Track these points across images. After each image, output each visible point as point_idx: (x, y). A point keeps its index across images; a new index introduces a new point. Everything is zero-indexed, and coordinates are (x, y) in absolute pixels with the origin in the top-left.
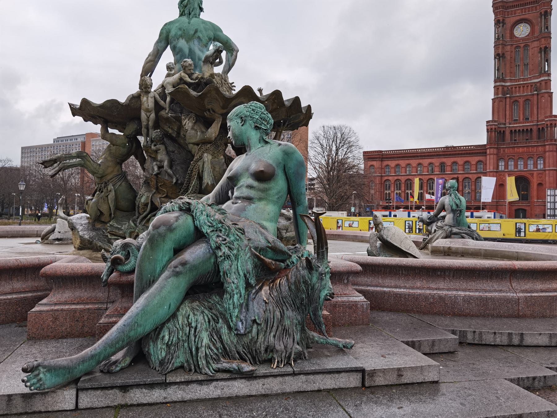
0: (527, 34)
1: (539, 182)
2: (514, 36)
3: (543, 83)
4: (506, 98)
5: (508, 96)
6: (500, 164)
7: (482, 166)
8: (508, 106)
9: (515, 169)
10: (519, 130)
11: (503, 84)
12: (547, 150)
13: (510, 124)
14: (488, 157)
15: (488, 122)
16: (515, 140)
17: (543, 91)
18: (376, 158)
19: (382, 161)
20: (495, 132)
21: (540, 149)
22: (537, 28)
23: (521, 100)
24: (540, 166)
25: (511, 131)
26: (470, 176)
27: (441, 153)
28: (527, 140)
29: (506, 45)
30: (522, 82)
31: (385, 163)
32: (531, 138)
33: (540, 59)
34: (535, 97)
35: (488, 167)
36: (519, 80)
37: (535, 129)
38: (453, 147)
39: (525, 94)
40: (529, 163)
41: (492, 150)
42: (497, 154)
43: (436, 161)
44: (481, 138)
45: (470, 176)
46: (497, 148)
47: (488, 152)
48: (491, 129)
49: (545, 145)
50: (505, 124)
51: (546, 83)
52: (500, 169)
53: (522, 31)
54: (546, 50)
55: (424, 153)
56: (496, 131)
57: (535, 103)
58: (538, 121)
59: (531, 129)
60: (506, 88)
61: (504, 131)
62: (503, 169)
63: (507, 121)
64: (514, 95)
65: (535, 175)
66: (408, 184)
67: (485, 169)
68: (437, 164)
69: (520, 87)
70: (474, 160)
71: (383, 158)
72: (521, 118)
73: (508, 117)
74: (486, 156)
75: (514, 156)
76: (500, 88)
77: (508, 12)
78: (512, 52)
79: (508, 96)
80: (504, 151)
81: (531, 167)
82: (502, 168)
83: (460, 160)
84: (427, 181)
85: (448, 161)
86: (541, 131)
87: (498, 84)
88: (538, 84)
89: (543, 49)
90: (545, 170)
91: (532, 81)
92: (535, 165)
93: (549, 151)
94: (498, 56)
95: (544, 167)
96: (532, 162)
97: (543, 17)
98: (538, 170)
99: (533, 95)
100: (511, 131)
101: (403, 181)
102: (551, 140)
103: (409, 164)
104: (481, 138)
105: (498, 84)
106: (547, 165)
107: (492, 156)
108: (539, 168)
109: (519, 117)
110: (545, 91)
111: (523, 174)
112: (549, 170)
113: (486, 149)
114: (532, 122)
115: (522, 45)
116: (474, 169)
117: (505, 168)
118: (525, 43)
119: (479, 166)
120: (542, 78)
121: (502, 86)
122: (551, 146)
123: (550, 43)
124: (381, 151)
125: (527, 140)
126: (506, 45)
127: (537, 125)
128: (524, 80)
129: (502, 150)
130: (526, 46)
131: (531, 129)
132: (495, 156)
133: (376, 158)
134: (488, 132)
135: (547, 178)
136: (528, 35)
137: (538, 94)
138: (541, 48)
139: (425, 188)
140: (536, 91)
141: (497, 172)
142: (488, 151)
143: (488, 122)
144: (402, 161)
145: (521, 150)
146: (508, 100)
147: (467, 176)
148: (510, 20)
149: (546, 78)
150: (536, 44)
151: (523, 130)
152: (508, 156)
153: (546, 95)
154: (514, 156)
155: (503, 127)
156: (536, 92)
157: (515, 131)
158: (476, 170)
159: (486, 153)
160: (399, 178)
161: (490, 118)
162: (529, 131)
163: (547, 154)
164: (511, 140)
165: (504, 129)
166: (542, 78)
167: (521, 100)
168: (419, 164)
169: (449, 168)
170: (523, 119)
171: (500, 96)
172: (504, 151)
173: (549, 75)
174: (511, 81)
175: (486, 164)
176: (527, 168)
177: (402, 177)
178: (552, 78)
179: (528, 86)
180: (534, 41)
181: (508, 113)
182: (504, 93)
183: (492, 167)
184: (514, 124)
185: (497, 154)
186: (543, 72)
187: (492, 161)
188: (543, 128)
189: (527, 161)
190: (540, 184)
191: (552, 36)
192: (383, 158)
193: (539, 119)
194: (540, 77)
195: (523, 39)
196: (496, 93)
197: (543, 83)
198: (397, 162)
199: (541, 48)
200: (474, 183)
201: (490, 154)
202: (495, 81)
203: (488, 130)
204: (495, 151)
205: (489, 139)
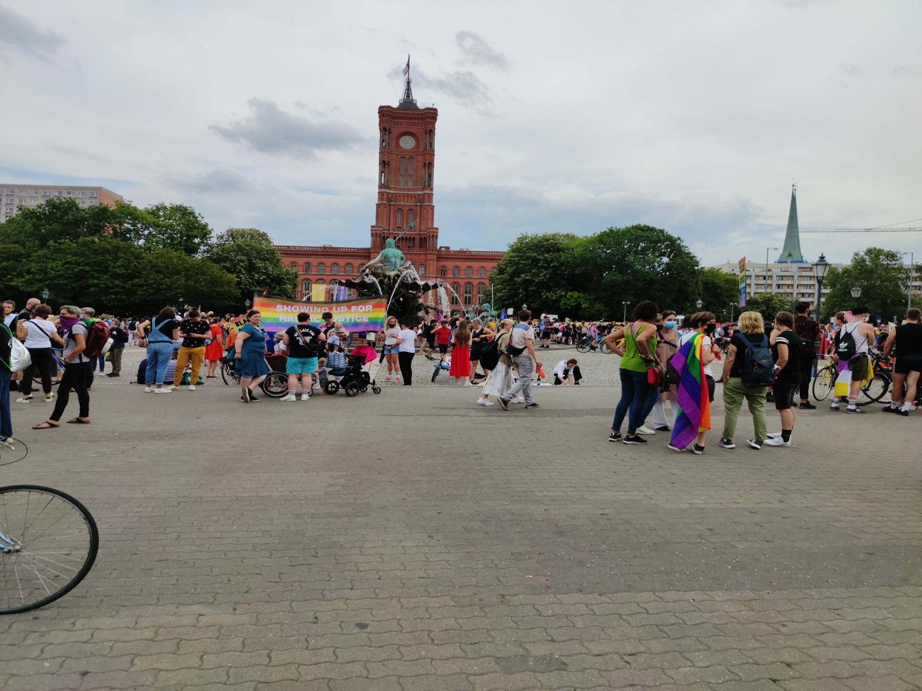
15: (372, 227)
21: (422, 257)
23: (405, 209)
34: (419, 208)
36: (403, 190)
37: (417, 238)
44: (366, 242)
53: (407, 143)
54: (430, 165)
70: (356, 262)
87: (383, 190)
94: (384, 164)
104: (366, 242)
105: (383, 190)
115: (407, 157)
118: (409, 156)
128: (408, 190)
146: (392, 207)
148: (396, 131)
161: (374, 224)
167: (405, 209)
174: (395, 189)
181: (392, 219)
182: (389, 200)
195: (408, 151)
202: (380, 187)
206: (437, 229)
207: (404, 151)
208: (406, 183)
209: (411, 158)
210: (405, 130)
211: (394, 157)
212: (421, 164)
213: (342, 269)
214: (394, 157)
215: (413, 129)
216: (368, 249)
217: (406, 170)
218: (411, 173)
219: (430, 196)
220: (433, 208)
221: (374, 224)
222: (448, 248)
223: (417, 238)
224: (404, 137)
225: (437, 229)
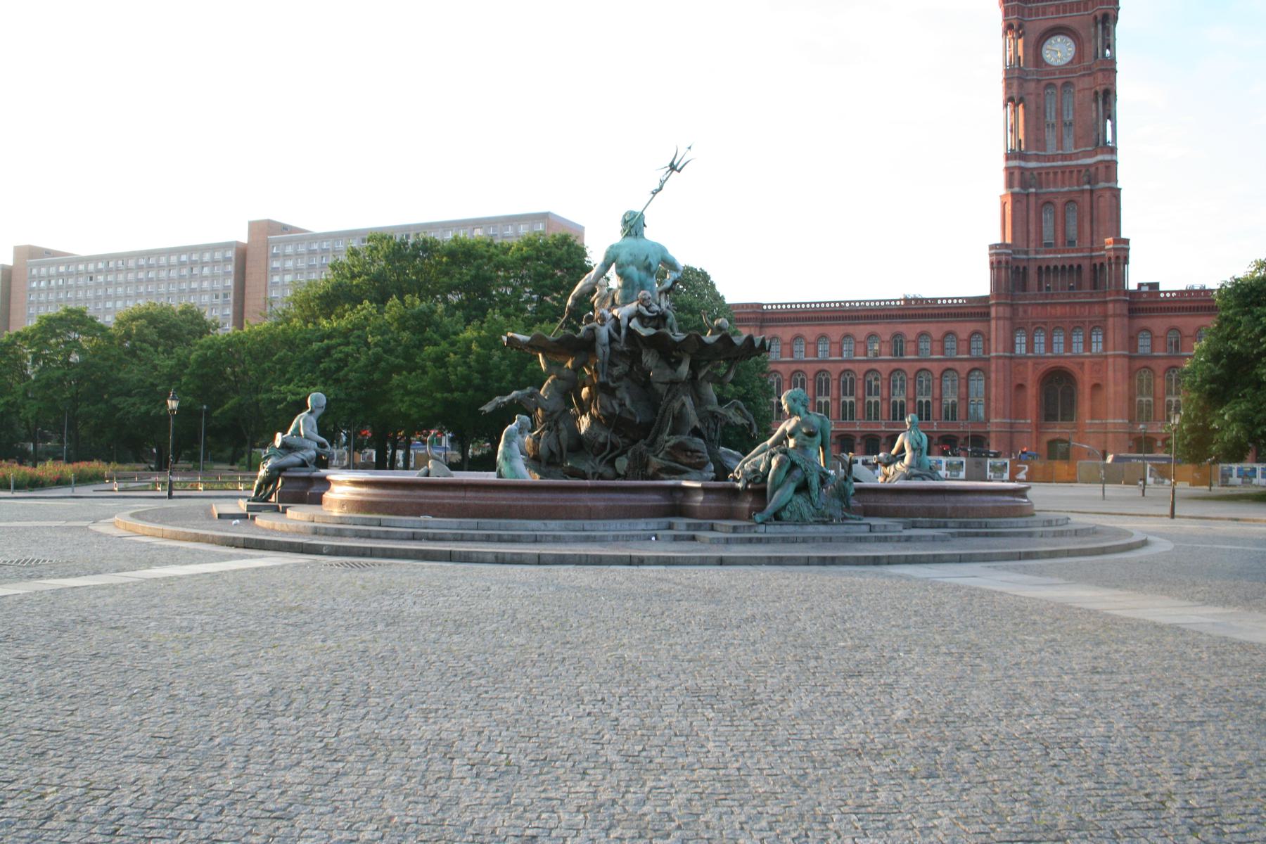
0: (1069, 59)
1: (1095, 381)
2: (1043, 61)
3: (1101, 167)
4: (1028, 195)
5: (1033, 190)
6: (1018, 340)
7: (980, 344)
8: (1032, 214)
9: (1046, 351)
10: (1056, 267)
11: (1023, 164)
12: (1110, 312)
13: (1037, 252)
14: (993, 323)
15: (992, 247)
16: (1048, 289)
17: (1102, 185)
18: (748, 320)
19: (761, 327)
20: (1007, 269)
22: (1089, 50)
23: (1059, 202)
24: (1097, 348)
25: (1040, 268)
26: (957, 365)
27: (895, 313)
28: (1071, 288)
29: (1026, 80)
30: (1060, 163)
31: (769, 333)
32: (1080, 286)
33: (1094, 115)
34: (1087, 196)
35: (993, 347)
37: (1086, 265)
38: (922, 300)
39: (1066, 189)
40: (1075, 339)
41: (1001, 309)
42: (1011, 319)
43: (885, 330)
44: (977, 282)
45: (957, 365)
46: (1012, 305)
47: (993, 314)
48: (999, 262)
49: (1106, 302)
50: (1027, 253)
51: (1107, 167)
52: (1018, 352)
53: (1059, 52)
54: (1107, 97)
55: (857, 310)
56: (1009, 266)
57: (1087, 208)
58: (1092, 250)
59: (1079, 266)
60: (1027, 173)
61: (1024, 268)
62: (1024, 352)
63: (1032, 245)
64: (1044, 190)
65: (1086, 366)
66: (820, 383)
67: (987, 350)
68: (887, 338)
69: (1055, 173)
70: (964, 329)
71: (763, 320)
72: (1060, 241)
73: (1032, 236)
74: (989, 321)
75: (1045, 323)
76: (1017, 173)
77: (1030, 9)
78: (1038, 95)
79: (1033, 190)
80: (1025, 312)
81: (1078, 349)
82: (1021, 349)
83: (936, 329)
84: (865, 375)
85: (910, 330)
86: (1098, 270)
88: (1093, 170)
89: (1100, 94)
90: (1106, 357)
91: (1080, 162)
92: (1088, 344)
93: (1115, 315)
95: (1105, 349)
96: (1081, 338)
97: (1100, 26)
98: (1091, 357)
99: (1083, 191)
100: (1040, 268)
101: (811, 376)
102: (1118, 293)
103: (823, 336)
104: (977, 282)
106: (1110, 344)
107: (1001, 323)
108: (1094, 350)
109: (1056, 239)
110: (1107, 185)
111: (1062, 363)
112: (1115, 356)
113: (989, 307)
114: (1081, 251)
115: (1059, 83)
116: (965, 349)
117: (1027, 351)
118: (1063, 79)
119: (974, 345)
120: (1099, 158)
121: (1020, 168)
122: (1117, 305)
123: (1114, 83)
124: (760, 305)
125: (1071, 288)
126: (1026, 80)
127: (1091, 258)
129: (1021, 309)
130: (1067, 84)
131: (1079, 266)
132: (1007, 323)
133: (748, 320)
134: (992, 268)
135: (1110, 373)
136: (1071, 62)
137: (1092, 191)
138: (1096, 93)
139: (860, 392)
140: (1089, 183)
141: (1011, 358)
142: (993, 310)
143: (992, 247)
144: (807, 329)
145: (1059, 311)
146: (1032, 199)
147: (949, 365)
148: (1039, 24)
149: (1108, 157)
150: (1086, 83)
151: (1063, 267)
152: (1034, 324)
153: (1108, 194)
154: (1045, 323)
155: (1023, 260)
156: (1087, 187)
157: (1048, 268)
158: (969, 352)
159: (988, 314)
160: (801, 367)
162: (1073, 270)
163: (1111, 321)
164: (1040, 289)
165: (1025, 264)
166: (1099, 158)
167: (1059, 202)
168: (847, 336)
169: (910, 347)
170: (1064, 244)
171: (1017, 189)
172: (1025, 312)
173: (1113, 150)
174: (1038, 158)
175: (989, 340)
176: (1070, 351)
177: (808, 366)
178: (1122, 157)
179: (1071, 172)
180: (1084, 75)
181: (1032, 228)
182: (1024, 184)
183: (1000, 348)
184: (1046, 253)
185: (1011, 319)
186: (1101, 143)
187: (1001, 333)
188: (1102, 264)
189: (1052, 336)
190: (1096, 387)
191: (1118, 68)
192: (763, 320)
193: (1095, 246)
194: (1096, 154)
195: (1061, 70)
196: (1009, 184)
197: (1101, 167)
198: (796, 331)
199: (1096, 93)
200: (963, 381)
201: (998, 318)
202: (1009, 156)
203: (992, 263)
204: (1007, 312)
205: (996, 283)
206: (1127, 241)
207: (1053, 70)
208: (1061, 141)
209: (1067, 84)
210: (1051, 24)
211: (1031, 86)
212: (1089, 95)
213: (937, 347)
214: (1031, 86)
215: (1068, 20)
216: (985, 299)
217: (1059, 113)
218: (1069, 117)
219: (1111, 167)
220: (1116, 193)
221: (998, 240)
222: (1154, 286)
223: (1086, 265)
224: (1052, 40)
225: (1127, 241)
